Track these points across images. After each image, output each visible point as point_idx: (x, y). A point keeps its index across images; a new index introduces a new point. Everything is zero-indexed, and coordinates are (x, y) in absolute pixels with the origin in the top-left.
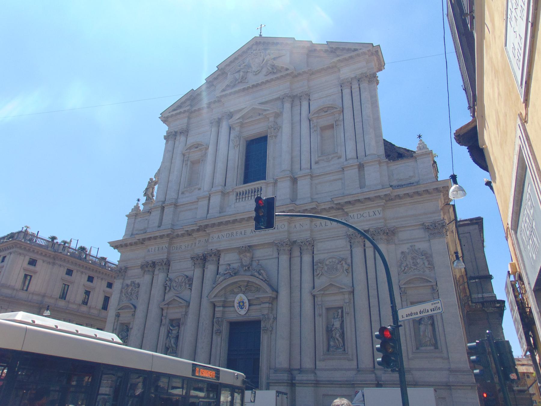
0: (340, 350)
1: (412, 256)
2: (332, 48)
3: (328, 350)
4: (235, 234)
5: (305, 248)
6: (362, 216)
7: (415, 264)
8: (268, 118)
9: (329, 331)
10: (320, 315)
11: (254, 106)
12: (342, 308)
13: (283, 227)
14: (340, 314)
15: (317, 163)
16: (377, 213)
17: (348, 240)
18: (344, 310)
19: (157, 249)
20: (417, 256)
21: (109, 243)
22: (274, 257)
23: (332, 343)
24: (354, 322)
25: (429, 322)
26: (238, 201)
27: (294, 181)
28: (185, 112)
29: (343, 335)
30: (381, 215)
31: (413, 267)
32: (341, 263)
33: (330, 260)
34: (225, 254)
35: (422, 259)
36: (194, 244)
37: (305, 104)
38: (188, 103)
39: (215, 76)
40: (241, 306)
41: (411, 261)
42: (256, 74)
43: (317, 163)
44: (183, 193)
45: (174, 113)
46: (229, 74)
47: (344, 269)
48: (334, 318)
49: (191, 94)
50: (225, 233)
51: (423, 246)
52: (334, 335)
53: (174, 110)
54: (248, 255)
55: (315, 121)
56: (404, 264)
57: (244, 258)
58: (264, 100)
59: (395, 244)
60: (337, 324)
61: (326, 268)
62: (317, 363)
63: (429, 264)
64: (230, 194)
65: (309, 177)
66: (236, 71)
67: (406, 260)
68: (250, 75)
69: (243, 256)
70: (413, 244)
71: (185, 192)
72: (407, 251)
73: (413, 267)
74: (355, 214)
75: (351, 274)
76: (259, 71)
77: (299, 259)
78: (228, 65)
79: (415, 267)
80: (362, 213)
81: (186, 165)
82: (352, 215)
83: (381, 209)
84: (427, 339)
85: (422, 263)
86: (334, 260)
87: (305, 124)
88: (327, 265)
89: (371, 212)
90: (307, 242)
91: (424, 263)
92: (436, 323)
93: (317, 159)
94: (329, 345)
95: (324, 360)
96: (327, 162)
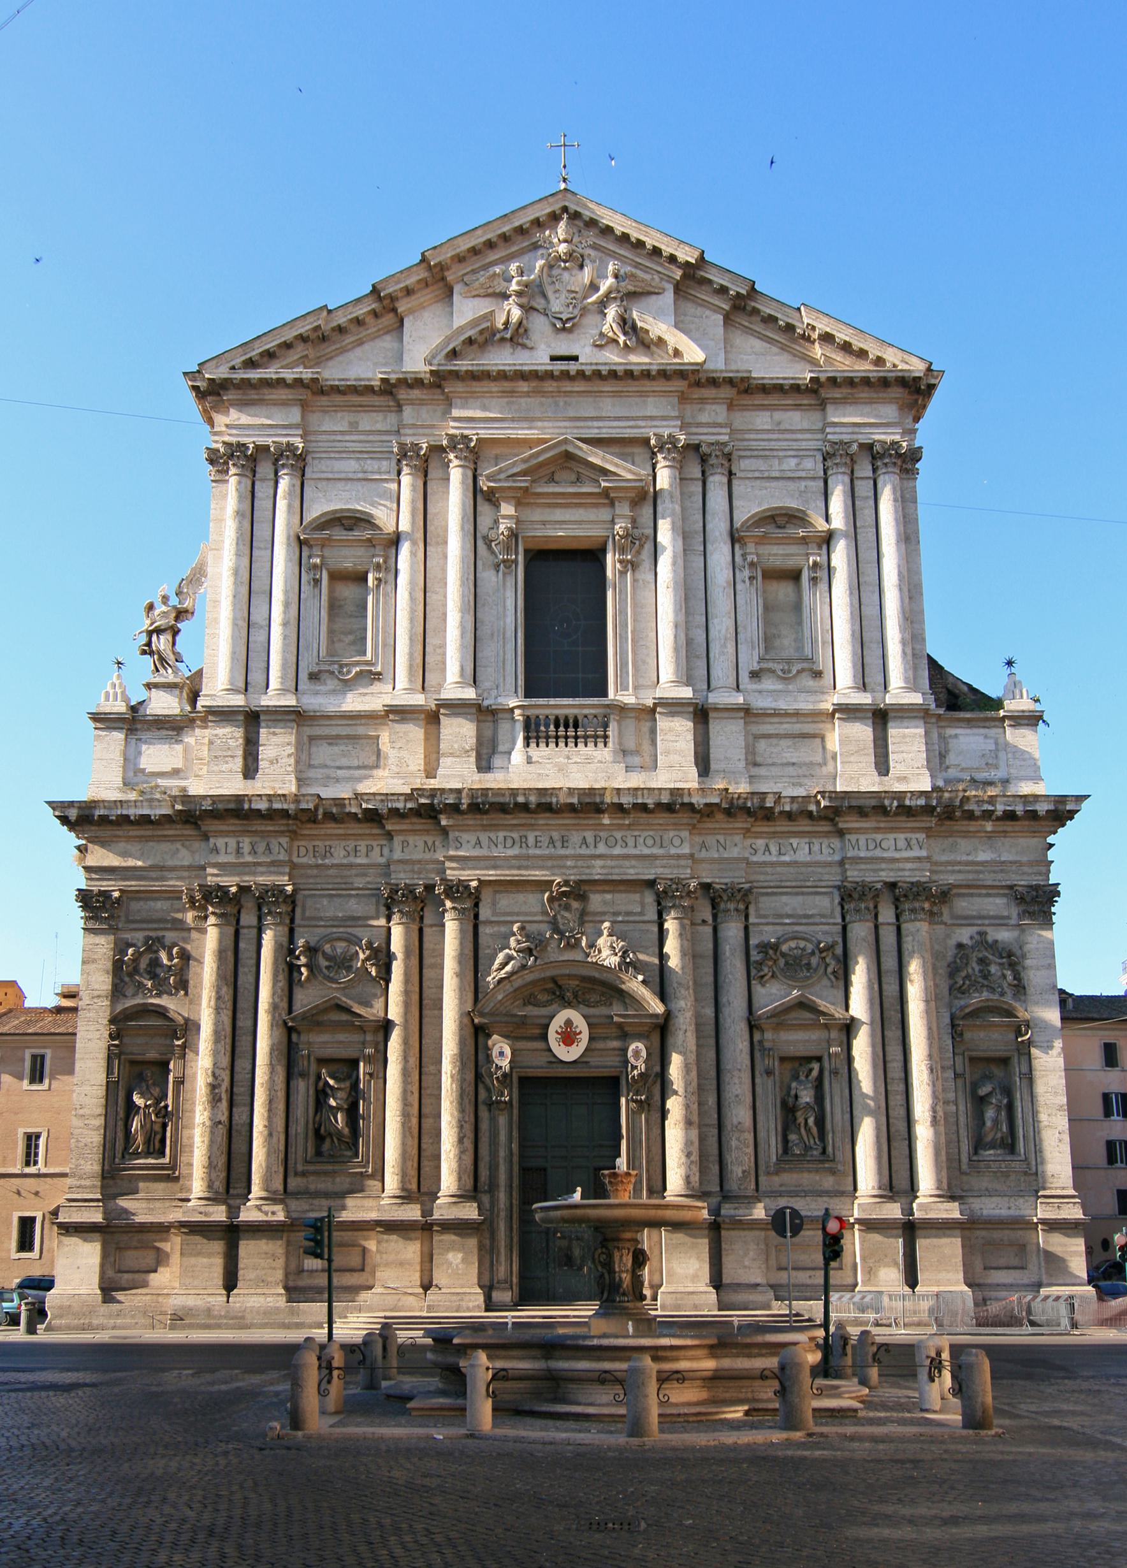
0: (815, 1153)
1: (980, 955)
2: (814, 328)
3: (786, 1150)
4: (531, 840)
5: (731, 906)
6: (878, 845)
7: (986, 975)
8: (612, 504)
9: (789, 1109)
10: (769, 1073)
11: (571, 449)
12: (819, 1059)
13: (677, 842)
14: (815, 1073)
15: (755, 675)
16: (914, 842)
17: (837, 900)
18: (826, 1065)
19: (246, 848)
20: (991, 957)
21: (49, 803)
22: (646, 918)
23: (793, 1137)
24: (847, 1091)
25: (1005, 1101)
26: (533, 745)
27: (701, 715)
28: (299, 382)
29: (821, 1122)
30: (924, 853)
31: (980, 980)
32: (824, 954)
33: (793, 944)
34: (496, 892)
35: (1000, 964)
36: (377, 850)
37: (717, 481)
38: (300, 350)
39: (411, 281)
40: (568, 1037)
41: (977, 968)
42: (564, 329)
43: (755, 675)
44: (314, 677)
45: (254, 375)
46: (457, 289)
47: (830, 970)
48: (796, 1077)
49: (320, 322)
50: (501, 834)
51: (1004, 936)
52: (801, 1120)
53: (250, 364)
54: (575, 905)
55: (751, 548)
56: (964, 974)
57: (562, 912)
58: (593, 433)
59: (945, 924)
60: (806, 1097)
61: (782, 962)
62: (762, 1179)
63: (1015, 979)
64: (500, 716)
65: (742, 714)
66: (490, 291)
67: (967, 964)
68: (539, 325)
69: (560, 905)
70: (984, 928)
71: (324, 676)
72: (970, 943)
73: (980, 980)
74: (862, 838)
75: (841, 983)
76: (576, 320)
77: (708, 930)
78: (460, 259)
79: (986, 983)
80: (879, 837)
81: (317, 582)
82: (853, 838)
83: (924, 836)
84: (999, 1135)
85: (999, 974)
86: (802, 944)
87: (720, 555)
88: (783, 955)
89: (901, 836)
90: (739, 891)
91: (1004, 976)
92: (1018, 1104)
93: (756, 667)
94: (786, 1141)
95: (777, 1173)
96: (785, 679)
